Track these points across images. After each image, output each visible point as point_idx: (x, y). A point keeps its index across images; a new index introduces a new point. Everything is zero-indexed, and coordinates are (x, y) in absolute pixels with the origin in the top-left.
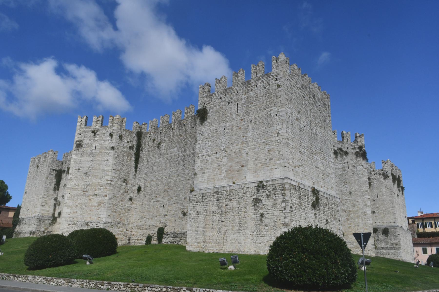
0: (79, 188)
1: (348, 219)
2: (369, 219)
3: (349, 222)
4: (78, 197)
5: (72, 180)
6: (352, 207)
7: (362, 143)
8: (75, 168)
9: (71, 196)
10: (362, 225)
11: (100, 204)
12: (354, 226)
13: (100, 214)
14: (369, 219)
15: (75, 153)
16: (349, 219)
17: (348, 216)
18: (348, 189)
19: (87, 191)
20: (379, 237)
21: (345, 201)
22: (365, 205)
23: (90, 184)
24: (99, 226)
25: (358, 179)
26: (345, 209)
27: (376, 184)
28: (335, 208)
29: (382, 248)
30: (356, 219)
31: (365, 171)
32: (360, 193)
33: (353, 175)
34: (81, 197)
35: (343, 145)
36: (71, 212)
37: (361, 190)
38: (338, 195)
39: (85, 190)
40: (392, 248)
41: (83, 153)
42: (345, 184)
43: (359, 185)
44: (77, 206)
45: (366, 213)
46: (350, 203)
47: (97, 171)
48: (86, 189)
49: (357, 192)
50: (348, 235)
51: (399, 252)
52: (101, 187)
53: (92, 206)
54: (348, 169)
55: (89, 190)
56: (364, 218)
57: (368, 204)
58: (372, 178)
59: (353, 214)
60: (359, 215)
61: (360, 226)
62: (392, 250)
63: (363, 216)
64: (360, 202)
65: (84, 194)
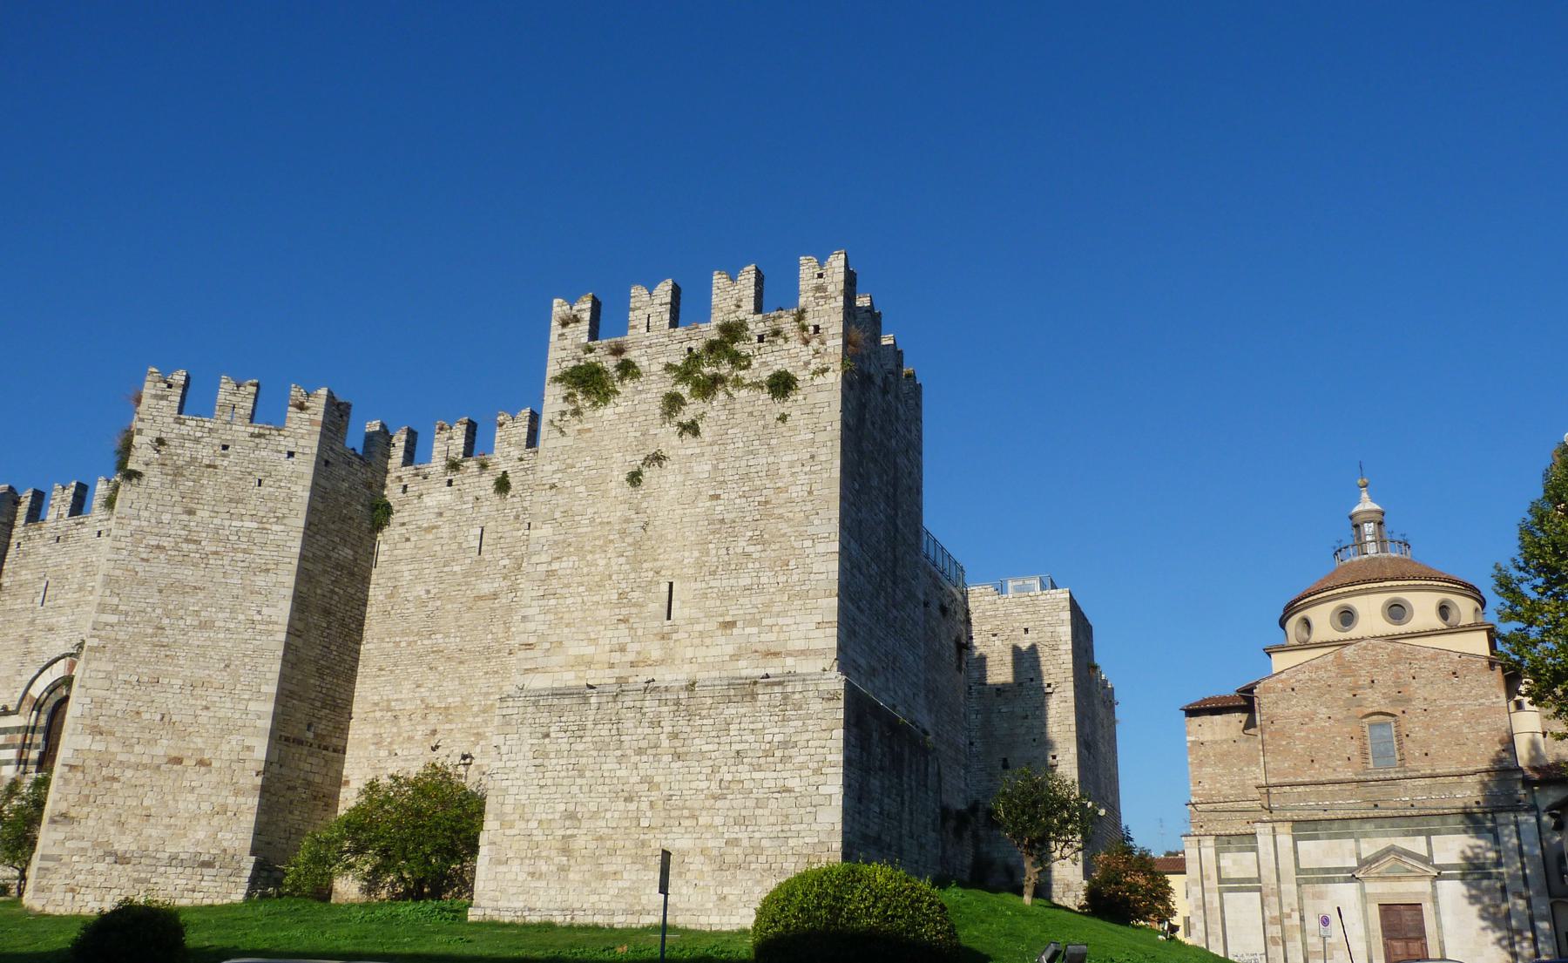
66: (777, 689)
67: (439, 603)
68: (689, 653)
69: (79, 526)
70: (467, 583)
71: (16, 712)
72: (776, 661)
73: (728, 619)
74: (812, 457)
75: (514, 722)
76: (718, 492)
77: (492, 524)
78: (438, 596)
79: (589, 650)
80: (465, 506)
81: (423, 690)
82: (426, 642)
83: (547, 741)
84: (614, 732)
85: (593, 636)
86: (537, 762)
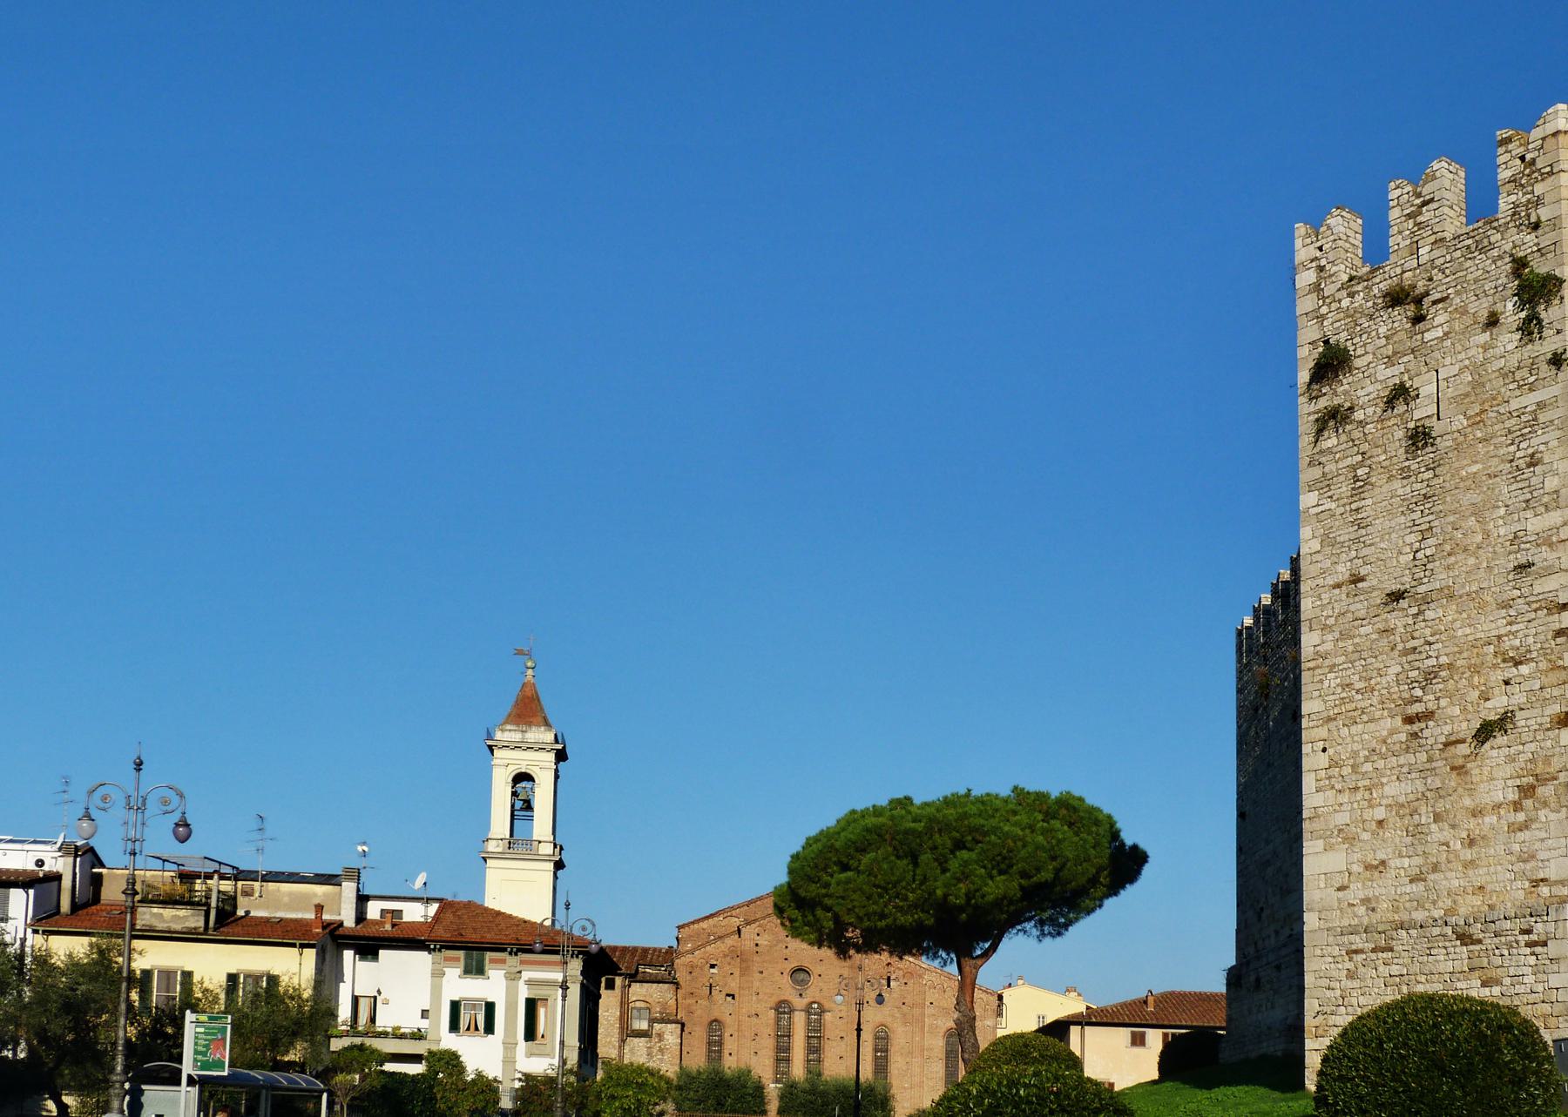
0: (1375, 701)
4: (1381, 764)
5: (1327, 662)
8: (1330, 581)
9: (1334, 764)
11: (1533, 787)
13: (1541, 855)
15: (1317, 481)
19: (1428, 715)
23: (1444, 660)
24: (1543, 938)
34: (1402, 760)
36: (1356, 868)
39: (1418, 708)
41: (1361, 464)
44: (1380, 823)
47: (1472, 561)
48: (1419, 700)
52: (1517, 664)
53: (1476, 813)
55: (1443, 703)
65: (1415, 735)
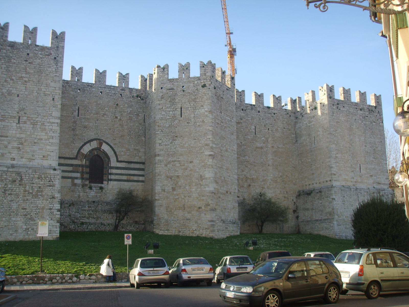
1: (174, 189)
2: (207, 185)
3: (175, 193)
6: (182, 171)
7: (207, 74)
10: (195, 195)
12: (183, 197)
14: (207, 185)
16: (176, 188)
17: (174, 184)
18: (178, 146)
20: (314, 204)
21: (172, 163)
22: (204, 166)
25: (195, 129)
26: (171, 175)
27: (314, 125)
28: (42, 182)
29: (317, 220)
30: (187, 188)
31: (208, 115)
32: (197, 149)
33: (188, 124)
35: (176, 84)
37: (199, 145)
38: (163, 156)
40: (325, 219)
42: (174, 140)
43: (195, 138)
45: (203, 177)
46: (179, 165)
49: (191, 149)
50: (173, 211)
51: (332, 225)
54: (181, 117)
56: (200, 184)
57: (209, 163)
58: (310, 117)
59: (183, 181)
60: (192, 182)
61: (192, 197)
62: (326, 223)
63: (199, 181)
64: (196, 161)
66: (383, 191)
67: (245, 147)
68: (365, 181)
69: (90, 87)
70: (253, 142)
71: (76, 158)
72: (380, 185)
73: (371, 175)
74: (381, 141)
75: (337, 193)
76: (366, 145)
77: (258, 126)
78: (245, 144)
79: (347, 177)
80: (249, 119)
81: (245, 172)
82: (243, 158)
83: (344, 198)
84: (357, 197)
85: (347, 174)
86: (343, 203)
